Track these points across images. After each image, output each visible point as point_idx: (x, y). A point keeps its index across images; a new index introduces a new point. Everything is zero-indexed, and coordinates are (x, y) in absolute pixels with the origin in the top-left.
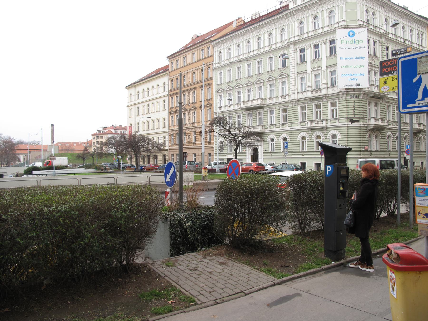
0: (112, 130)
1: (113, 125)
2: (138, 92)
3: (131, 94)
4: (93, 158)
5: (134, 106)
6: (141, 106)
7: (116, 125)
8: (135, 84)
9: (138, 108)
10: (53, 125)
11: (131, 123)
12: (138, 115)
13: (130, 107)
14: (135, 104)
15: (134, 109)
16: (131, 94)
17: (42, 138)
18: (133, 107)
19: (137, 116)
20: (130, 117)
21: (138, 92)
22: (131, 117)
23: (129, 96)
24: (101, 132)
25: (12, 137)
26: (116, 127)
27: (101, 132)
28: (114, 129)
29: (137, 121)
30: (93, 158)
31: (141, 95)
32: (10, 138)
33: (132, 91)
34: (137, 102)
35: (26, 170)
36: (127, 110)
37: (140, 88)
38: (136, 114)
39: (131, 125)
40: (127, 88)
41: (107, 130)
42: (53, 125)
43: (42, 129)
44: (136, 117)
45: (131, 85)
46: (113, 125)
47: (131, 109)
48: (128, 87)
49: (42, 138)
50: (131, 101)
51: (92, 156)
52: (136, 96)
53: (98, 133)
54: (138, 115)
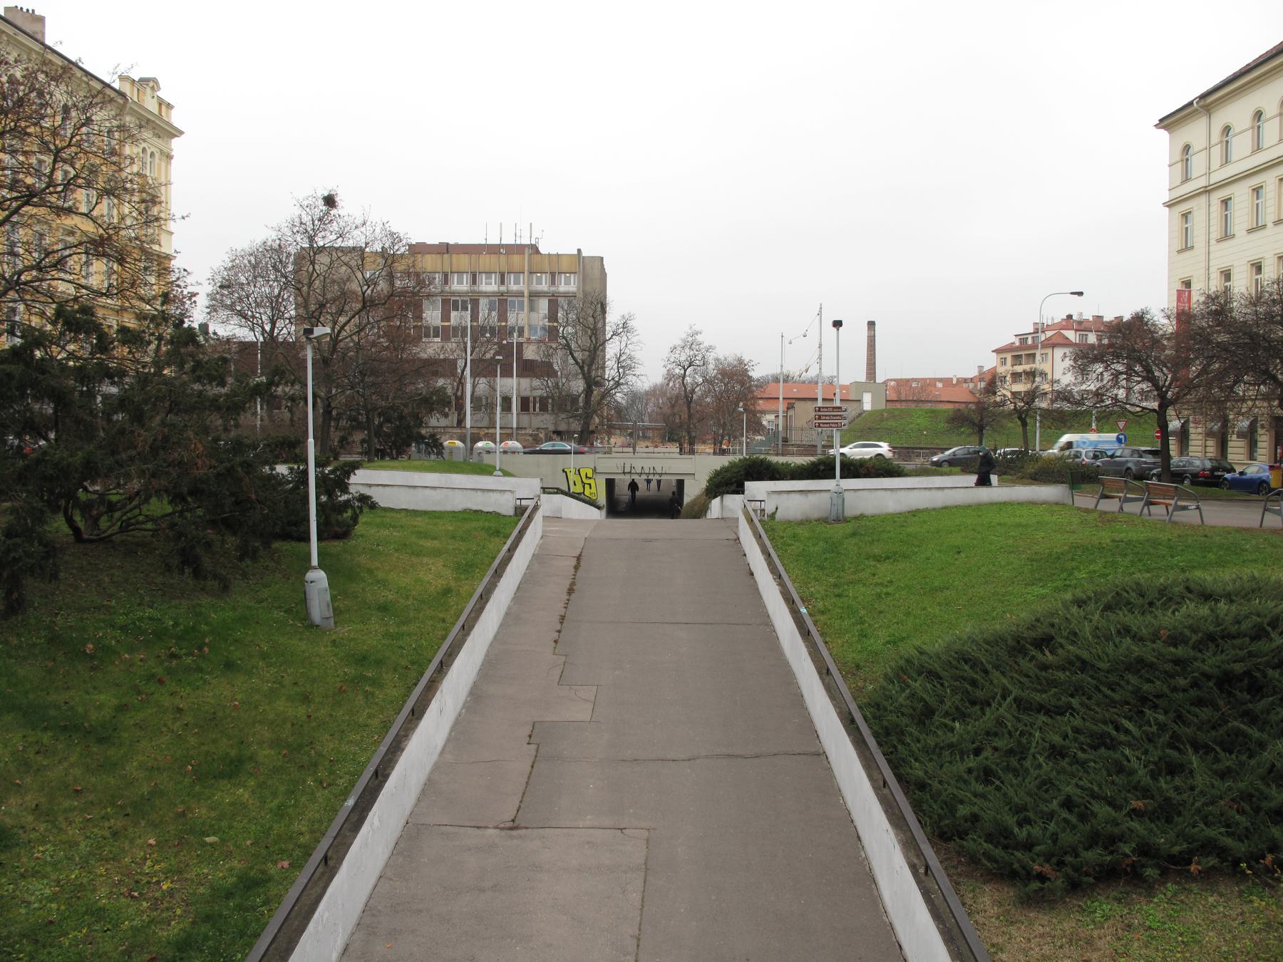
0: (1062, 331)
1: (1070, 317)
2: (1227, 130)
3: (1187, 148)
4: (1024, 424)
5: (1203, 199)
6: (1241, 194)
7: (1081, 314)
8: (1208, 102)
9: (1226, 202)
10: (871, 324)
11: (1185, 275)
12: (1227, 236)
13: (1184, 207)
14: (1207, 191)
15: (1205, 214)
16: (1187, 148)
17: (820, 347)
18: (1198, 206)
19: (1219, 241)
20: (1179, 252)
21: (1227, 130)
22: (1187, 248)
23: (1178, 157)
24: (1030, 342)
25: (746, 359)
26: (1080, 323)
27: (1030, 342)
28: (1076, 330)
29: (1218, 263)
30: (1024, 424)
31: (1241, 144)
32: (740, 361)
33: (1195, 132)
34: (1215, 178)
35: (717, 474)
36: (1161, 223)
37: (1237, 113)
38: (1216, 232)
39: (1188, 284)
40: (1165, 128)
41: (1049, 334)
42: (871, 324)
43: (820, 314)
44: (1215, 247)
45: (1191, 104)
46: (1070, 317)
47: (1185, 216)
48: (1169, 122)
49: (820, 347)
50: (1186, 179)
51: (1020, 418)
52: (1217, 152)
53: (1017, 344)
54: (1227, 236)
